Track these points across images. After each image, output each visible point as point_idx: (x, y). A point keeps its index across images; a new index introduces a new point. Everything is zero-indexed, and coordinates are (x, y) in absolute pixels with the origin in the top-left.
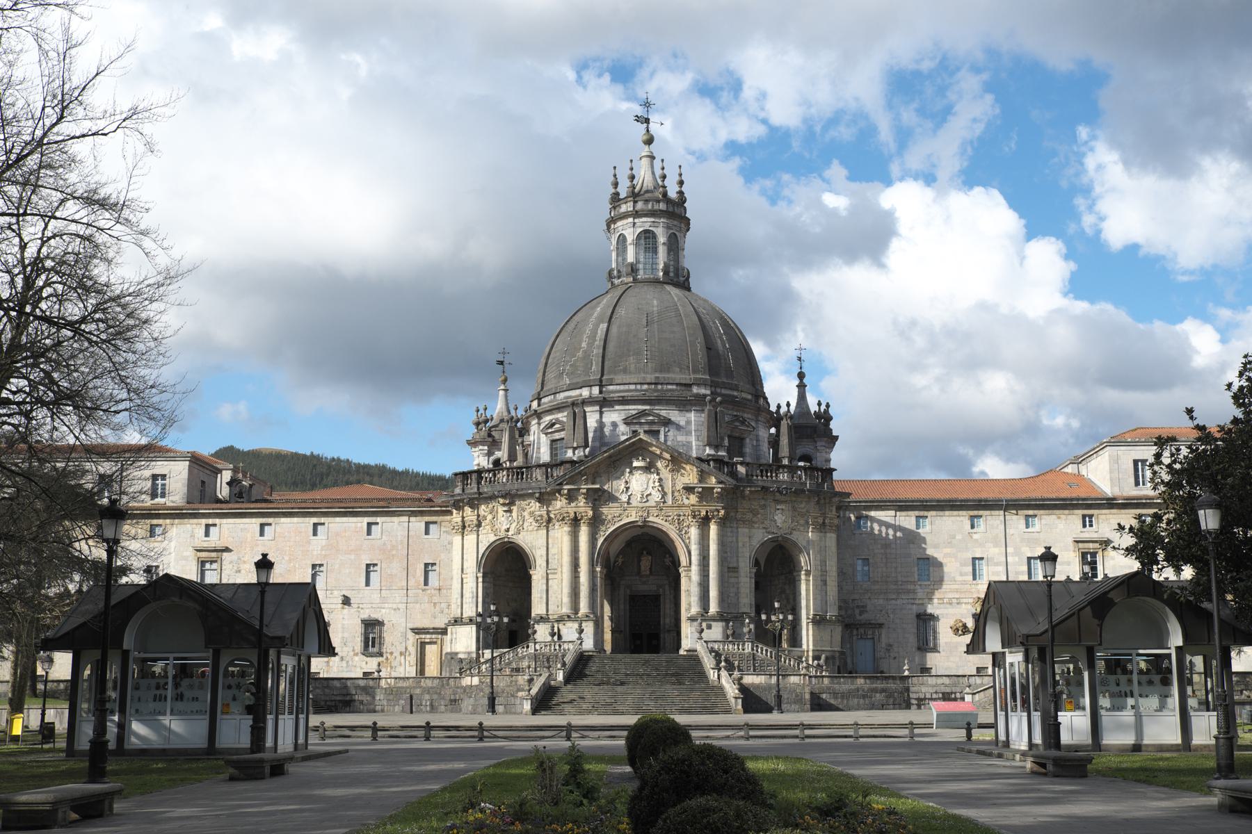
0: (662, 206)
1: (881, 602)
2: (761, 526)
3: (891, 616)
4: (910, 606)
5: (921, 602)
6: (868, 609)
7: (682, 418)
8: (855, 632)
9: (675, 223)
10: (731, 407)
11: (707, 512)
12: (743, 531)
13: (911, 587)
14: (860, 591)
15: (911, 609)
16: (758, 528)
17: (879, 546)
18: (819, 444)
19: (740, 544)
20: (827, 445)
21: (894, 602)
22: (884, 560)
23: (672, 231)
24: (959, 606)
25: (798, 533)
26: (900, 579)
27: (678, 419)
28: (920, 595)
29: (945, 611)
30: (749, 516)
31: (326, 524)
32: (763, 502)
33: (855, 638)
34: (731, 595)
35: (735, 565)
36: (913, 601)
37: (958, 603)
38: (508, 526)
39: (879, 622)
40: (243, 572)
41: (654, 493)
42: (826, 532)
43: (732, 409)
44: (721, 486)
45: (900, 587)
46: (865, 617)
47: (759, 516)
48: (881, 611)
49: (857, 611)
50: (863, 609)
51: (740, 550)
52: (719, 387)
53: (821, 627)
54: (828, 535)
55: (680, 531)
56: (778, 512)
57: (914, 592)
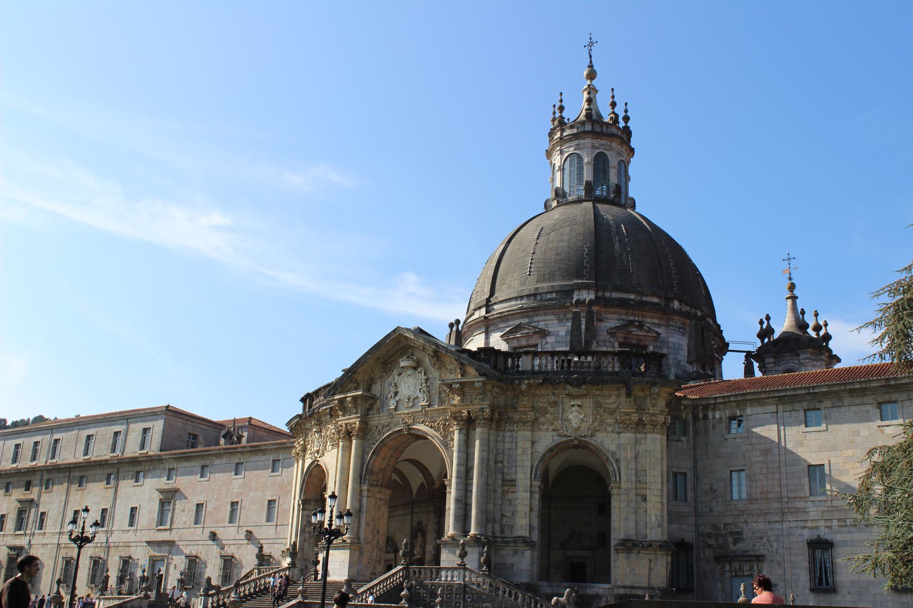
0: (588, 127)
1: (761, 526)
2: (551, 428)
3: (775, 545)
4: (799, 531)
5: (814, 524)
6: (745, 535)
7: (561, 328)
8: (727, 567)
9: (604, 142)
10: (622, 311)
11: (469, 412)
12: (524, 435)
13: (800, 505)
14: (735, 513)
15: (801, 535)
16: (547, 430)
17: (758, 453)
18: (802, 356)
19: (519, 451)
20: (815, 357)
21: (778, 526)
22: (764, 471)
23: (599, 151)
24: (869, 529)
25: (604, 434)
26: (785, 494)
27: (558, 329)
28: (812, 515)
29: (849, 537)
30: (531, 416)
31: (244, 463)
32: (553, 399)
33: (728, 575)
34: (508, 514)
35: (514, 477)
36: (803, 524)
37: (867, 526)
38: (318, 449)
39: (758, 553)
40: (186, 511)
41: (420, 395)
42: (646, 433)
43: (627, 314)
44: (481, 379)
45: (786, 505)
46: (741, 546)
47: (548, 415)
48: (761, 538)
49: (730, 540)
50: (738, 536)
51: (519, 458)
52: (607, 291)
53: (633, 556)
54: (649, 436)
55: (445, 437)
56: (573, 409)
57: (805, 511)
